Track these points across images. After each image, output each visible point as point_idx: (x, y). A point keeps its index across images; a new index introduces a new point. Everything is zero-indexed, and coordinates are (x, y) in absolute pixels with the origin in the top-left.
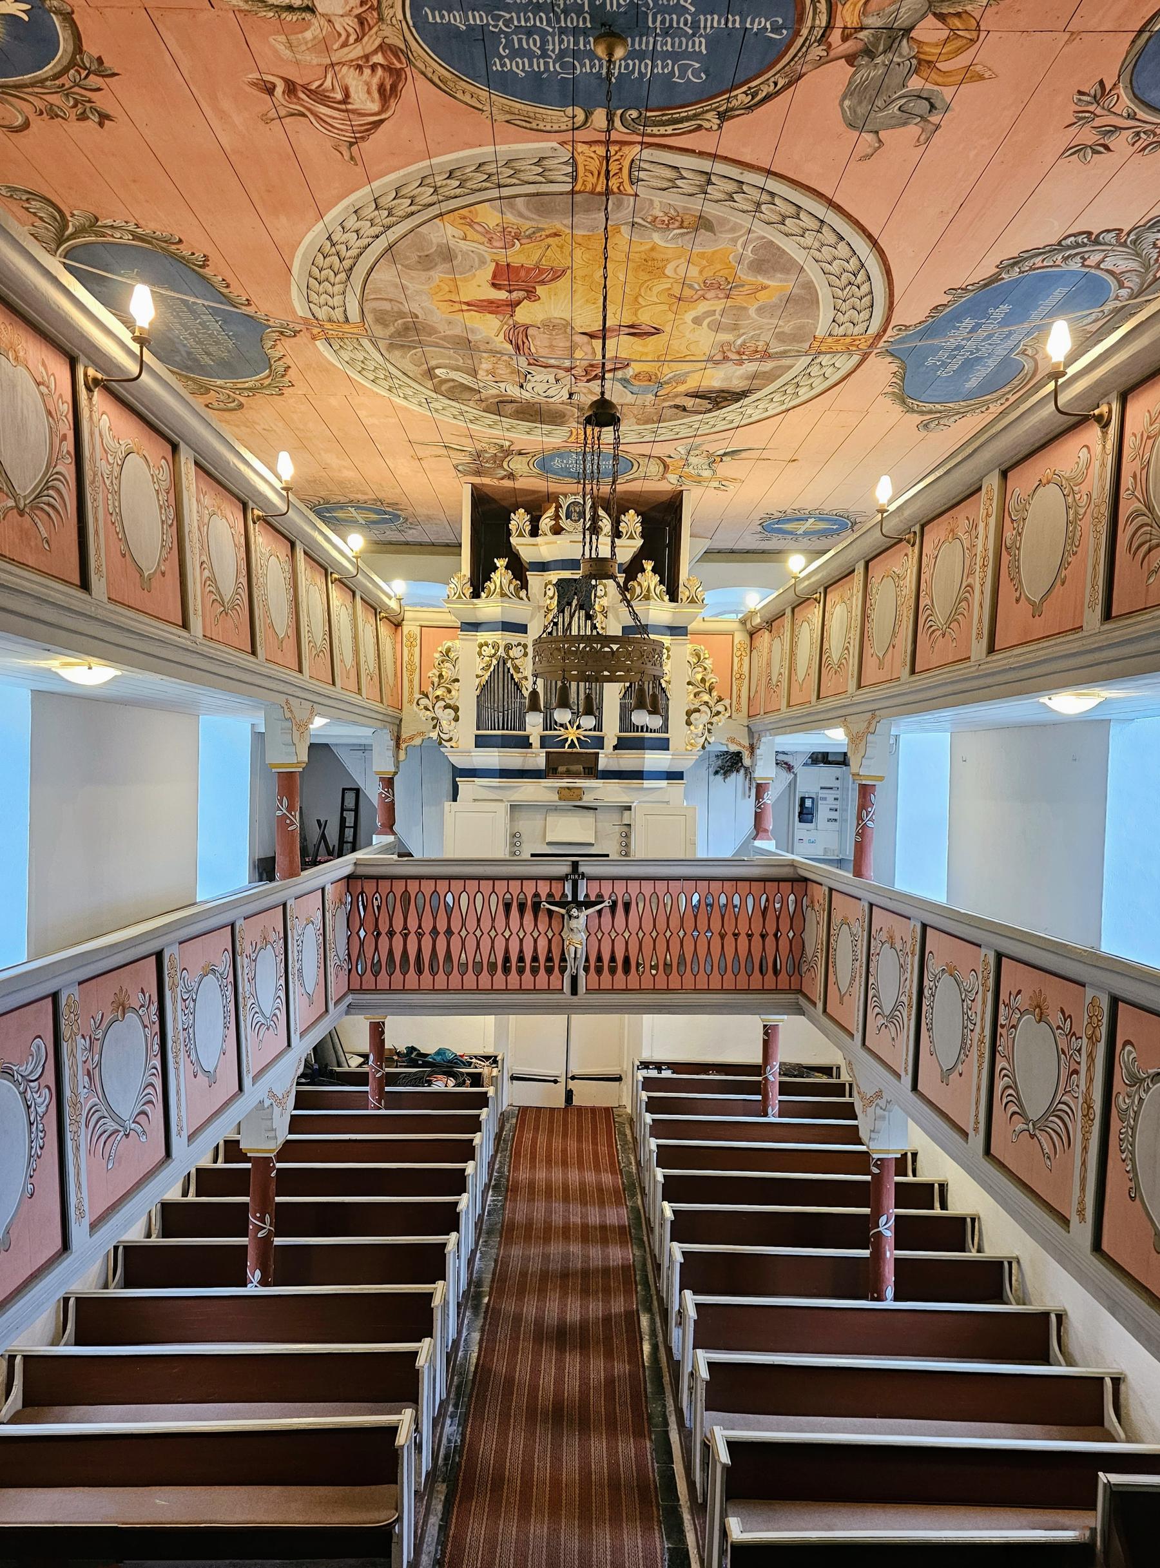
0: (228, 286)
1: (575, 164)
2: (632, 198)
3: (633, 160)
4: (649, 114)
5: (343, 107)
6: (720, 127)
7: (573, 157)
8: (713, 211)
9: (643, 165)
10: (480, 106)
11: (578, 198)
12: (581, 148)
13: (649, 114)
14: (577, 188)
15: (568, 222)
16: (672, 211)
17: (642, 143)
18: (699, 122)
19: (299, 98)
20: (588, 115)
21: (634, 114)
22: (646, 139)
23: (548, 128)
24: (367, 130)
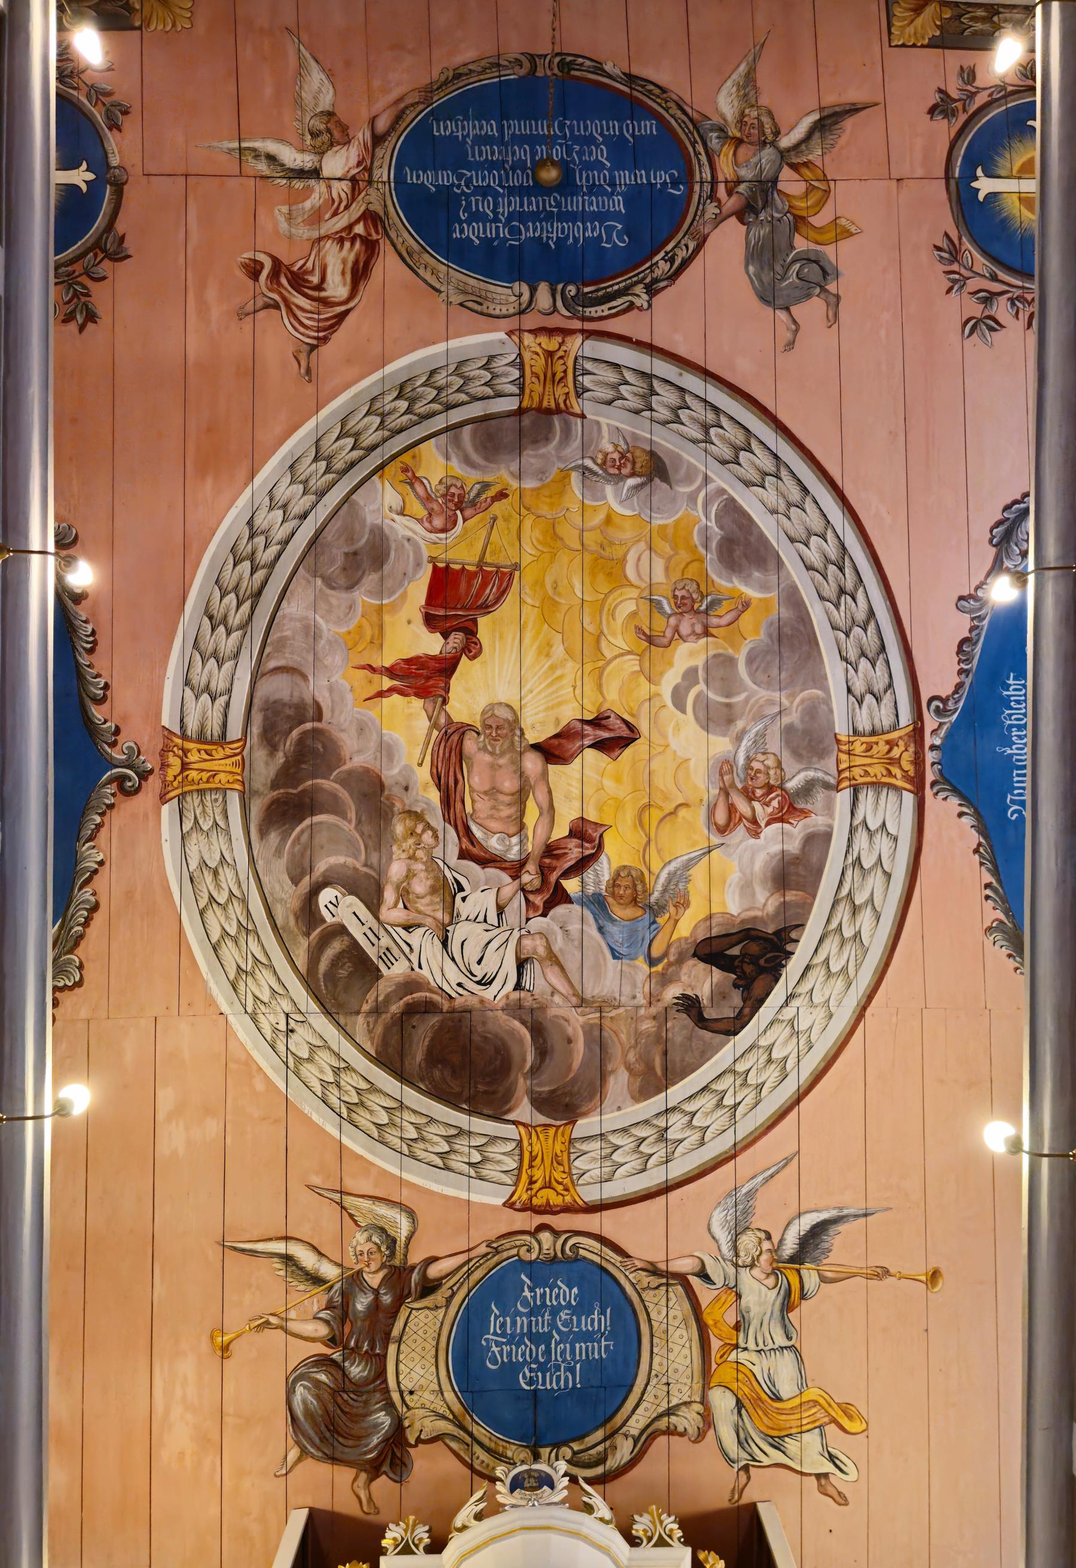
0: (91, 651)
1: (521, 367)
2: (579, 421)
3: (576, 358)
4: (586, 290)
5: (315, 294)
6: (650, 306)
7: (520, 355)
8: (666, 441)
9: (589, 366)
10: (437, 285)
11: (527, 421)
12: (528, 339)
13: (586, 290)
14: (525, 404)
15: (514, 467)
16: (622, 443)
17: (582, 331)
18: (630, 298)
19: (280, 284)
20: (533, 291)
21: (572, 290)
22: (588, 326)
23: (497, 312)
24: (332, 326)
